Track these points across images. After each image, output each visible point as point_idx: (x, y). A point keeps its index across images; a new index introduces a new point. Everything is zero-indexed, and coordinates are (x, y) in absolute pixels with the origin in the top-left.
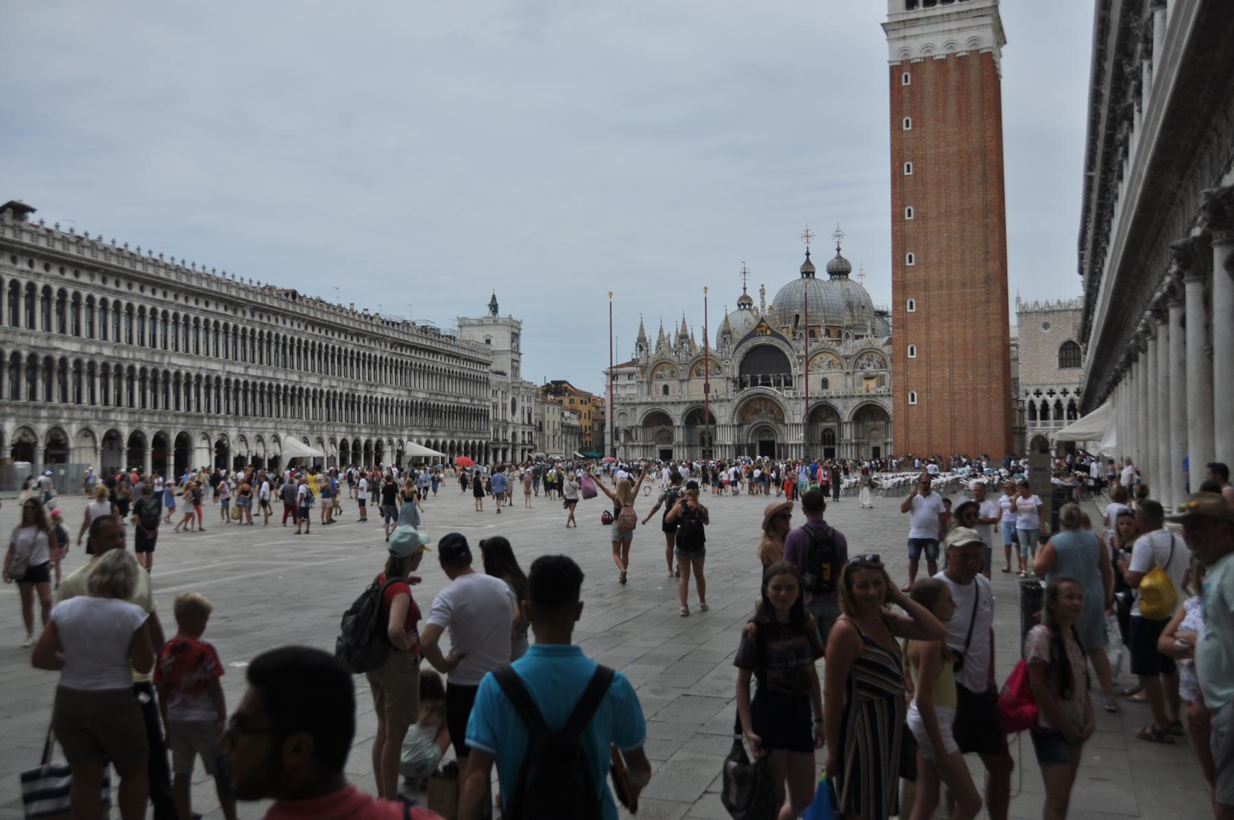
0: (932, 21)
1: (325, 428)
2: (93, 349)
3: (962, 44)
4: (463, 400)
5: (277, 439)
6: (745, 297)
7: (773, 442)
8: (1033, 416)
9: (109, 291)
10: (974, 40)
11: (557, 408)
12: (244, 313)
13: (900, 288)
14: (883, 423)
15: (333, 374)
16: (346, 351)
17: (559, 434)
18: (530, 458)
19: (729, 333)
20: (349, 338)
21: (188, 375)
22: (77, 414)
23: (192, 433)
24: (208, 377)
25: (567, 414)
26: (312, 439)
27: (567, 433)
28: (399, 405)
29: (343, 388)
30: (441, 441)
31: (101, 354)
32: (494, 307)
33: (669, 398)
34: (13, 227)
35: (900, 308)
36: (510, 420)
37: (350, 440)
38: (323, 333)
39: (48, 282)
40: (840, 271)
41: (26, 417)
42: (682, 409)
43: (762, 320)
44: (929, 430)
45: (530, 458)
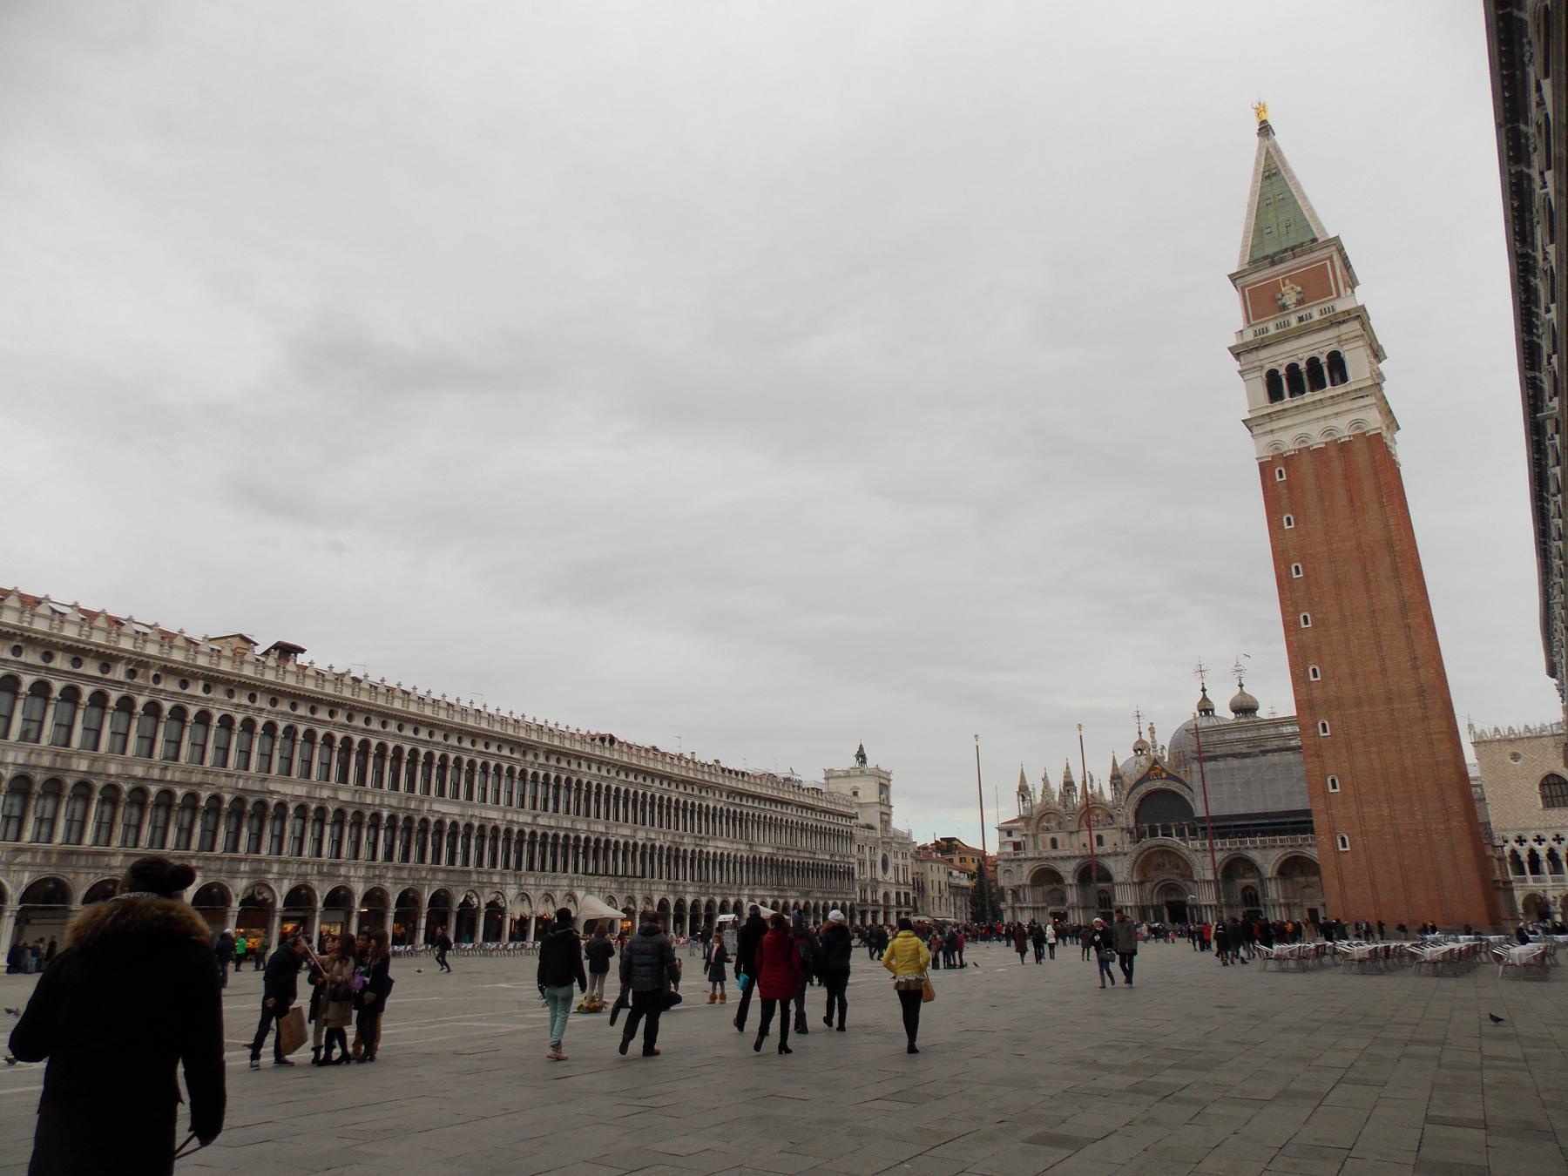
1: (638, 886)
2: (325, 793)
3: (1343, 428)
5: (572, 897)
6: (1141, 741)
7: (1183, 904)
9: (355, 729)
11: (942, 867)
12: (536, 756)
14: (1316, 879)
16: (669, 800)
17: (946, 895)
19: (1119, 777)
21: (454, 824)
22: (292, 868)
23: (454, 891)
24: (482, 827)
25: (955, 873)
26: (621, 900)
28: (739, 862)
29: (662, 839)
30: (792, 902)
31: (335, 799)
32: (861, 756)
34: (276, 669)
35: (1310, 731)
37: (672, 900)
38: (640, 780)
39: (272, 717)
40: (1245, 708)
41: (220, 871)
44: (1373, 885)
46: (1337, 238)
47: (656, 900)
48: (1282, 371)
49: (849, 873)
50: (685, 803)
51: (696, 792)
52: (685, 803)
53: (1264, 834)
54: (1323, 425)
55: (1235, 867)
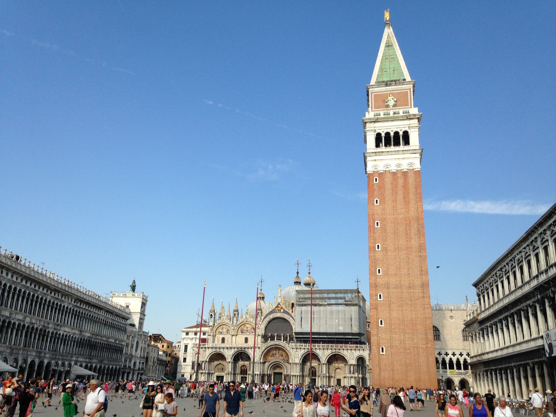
1: (21, 352)
4: (111, 340)
7: (281, 373)
10: (410, 164)
11: (156, 349)
14: (343, 365)
15: (34, 314)
18: (141, 378)
19: (261, 310)
20: (49, 292)
25: (161, 353)
27: (160, 364)
28: (73, 340)
29: (38, 325)
35: (374, 298)
36: (134, 355)
37: (37, 361)
38: (33, 286)
42: (232, 352)
43: (279, 304)
45: (141, 378)
47: (29, 361)
48: (383, 135)
50: (53, 303)
51: (60, 297)
52: (53, 303)
53: (324, 342)
55: (308, 357)
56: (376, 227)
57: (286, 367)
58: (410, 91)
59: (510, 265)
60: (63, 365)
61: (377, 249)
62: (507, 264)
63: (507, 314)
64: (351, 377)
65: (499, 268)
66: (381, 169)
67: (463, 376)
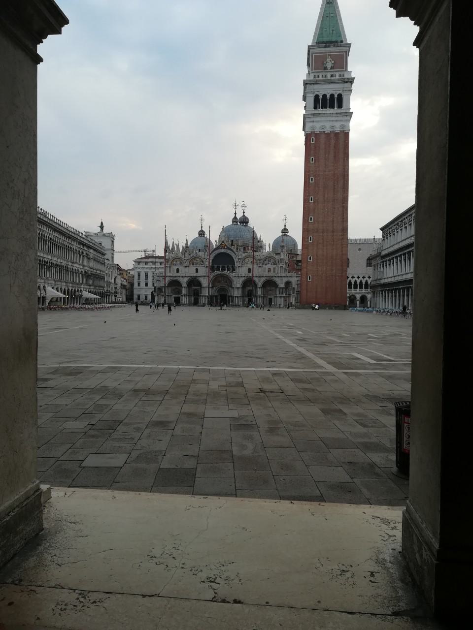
0: (326, 115)
4: (98, 272)
5: (44, 287)
8: (350, 287)
13: (306, 231)
14: (274, 288)
27: (123, 288)
32: (102, 227)
33: (181, 274)
38: (58, 236)
40: (245, 221)
42: (186, 279)
43: (223, 242)
46: (350, 44)
48: (321, 97)
49: (103, 278)
54: (331, 124)
56: (311, 182)
57: (230, 290)
58: (346, 54)
59: (408, 219)
60: (78, 290)
61: (310, 201)
62: (407, 218)
63: (402, 253)
64: (280, 297)
65: (400, 220)
66: (318, 130)
67: (363, 294)
